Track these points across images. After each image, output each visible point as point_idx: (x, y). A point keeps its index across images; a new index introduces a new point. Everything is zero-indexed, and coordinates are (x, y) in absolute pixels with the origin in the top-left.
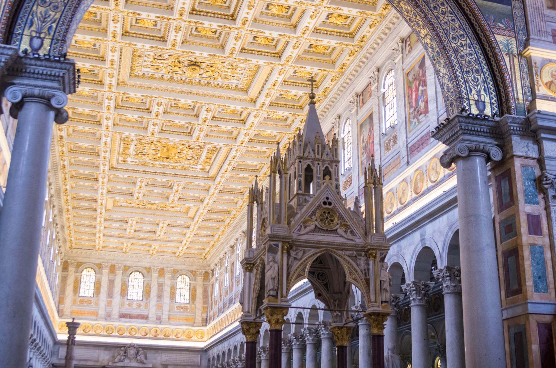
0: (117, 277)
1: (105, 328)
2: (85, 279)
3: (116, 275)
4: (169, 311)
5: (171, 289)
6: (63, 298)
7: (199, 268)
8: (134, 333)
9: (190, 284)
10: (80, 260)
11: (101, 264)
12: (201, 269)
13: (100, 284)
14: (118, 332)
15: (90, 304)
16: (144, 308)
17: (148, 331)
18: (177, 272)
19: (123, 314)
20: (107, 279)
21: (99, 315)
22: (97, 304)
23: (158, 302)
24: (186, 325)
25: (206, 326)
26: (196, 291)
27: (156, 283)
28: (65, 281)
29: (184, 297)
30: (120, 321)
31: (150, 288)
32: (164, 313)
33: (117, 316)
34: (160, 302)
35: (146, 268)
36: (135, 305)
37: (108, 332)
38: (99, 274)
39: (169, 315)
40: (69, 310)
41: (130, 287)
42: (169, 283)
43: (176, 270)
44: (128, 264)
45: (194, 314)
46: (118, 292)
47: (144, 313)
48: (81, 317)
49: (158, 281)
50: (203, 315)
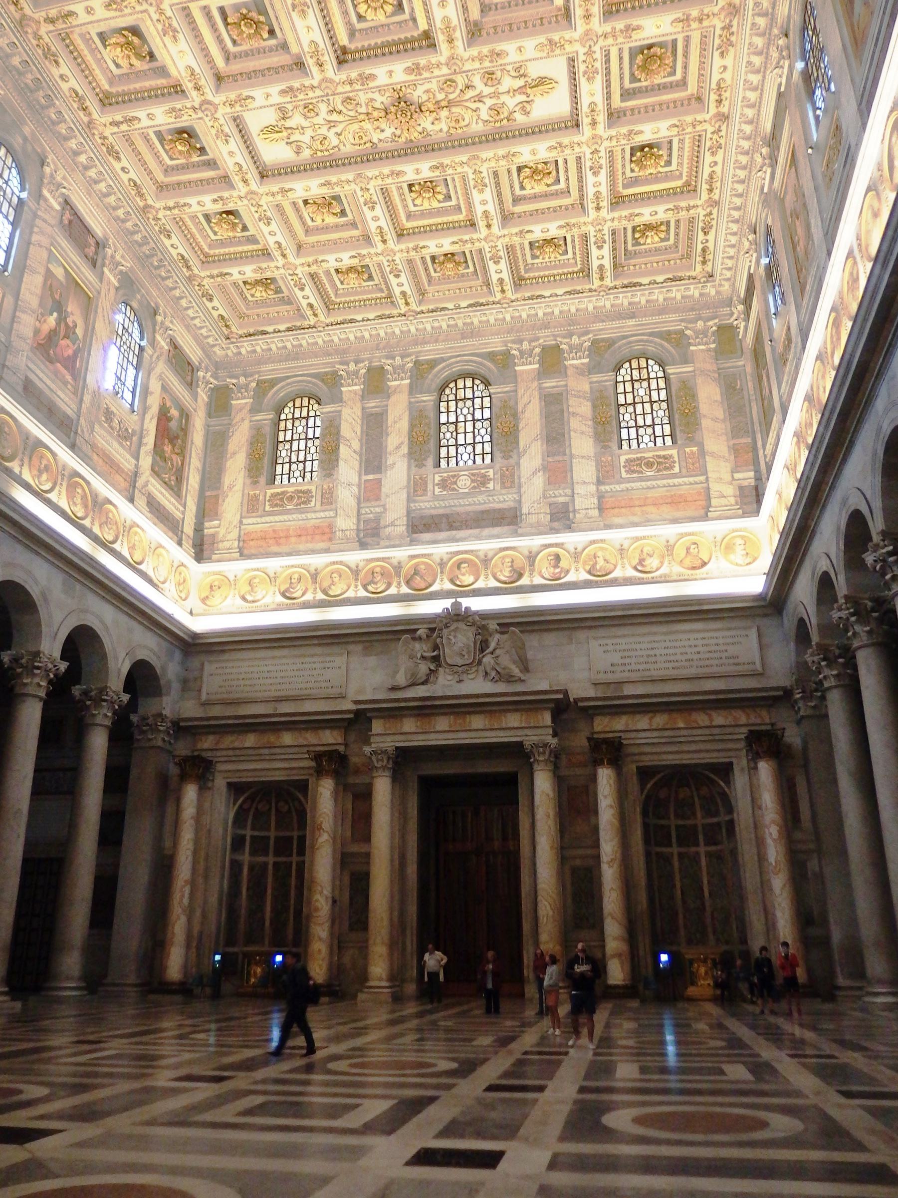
0: (393, 399)
1: (362, 574)
2: (289, 433)
3: (389, 397)
4: (599, 482)
5: (594, 407)
6: (217, 497)
7: (692, 315)
8: (468, 579)
9: (666, 378)
10: (269, 371)
11: (335, 373)
12: (700, 318)
13: (338, 433)
14: (408, 583)
15: (304, 503)
16: (498, 487)
17: (521, 561)
18: (610, 346)
19: (422, 517)
20: (359, 413)
21: (339, 534)
22: (328, 499)
23: (550, 459)
24: (675, 521)
25: (757, 512)
26: (694, 396)
27: (536, 394)
28: (222, 445)
29: (650, 431)
30: (412, 542)
31: (515, 416)
32: (578, 489)
33: (401, 529)
34: (557, 458)
35: (491, 356)
36: (464, 483)
37: (370, 588)
38: (333, 402)
39: (601, 497)
40: (234, 534)
41: (444, 429)
42: (587, 387)
43: (603, 340)
44: (429, 352)
45: (702, 478)
46: (398, 447)
47: (503, 500)
48: (275, 549)
49: (540, 388)
50: (737, 476)
